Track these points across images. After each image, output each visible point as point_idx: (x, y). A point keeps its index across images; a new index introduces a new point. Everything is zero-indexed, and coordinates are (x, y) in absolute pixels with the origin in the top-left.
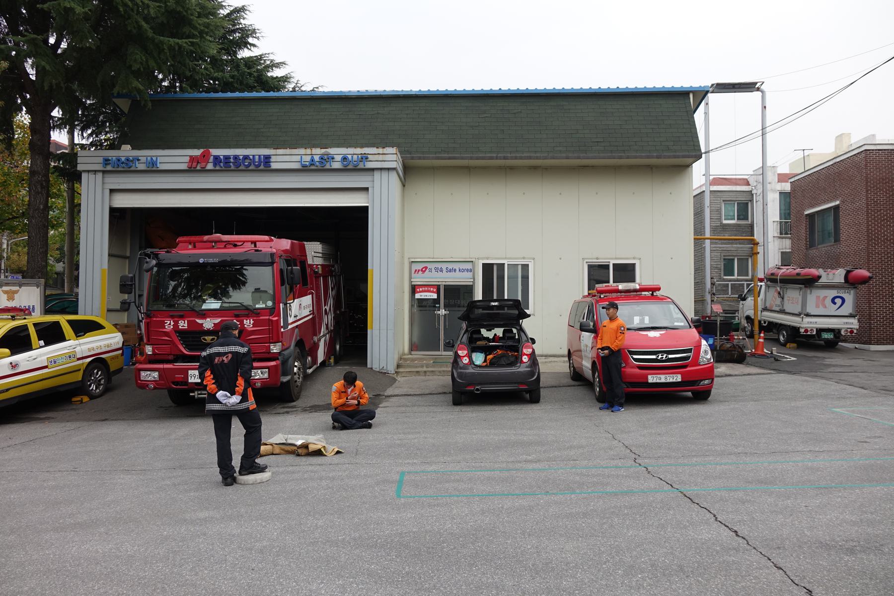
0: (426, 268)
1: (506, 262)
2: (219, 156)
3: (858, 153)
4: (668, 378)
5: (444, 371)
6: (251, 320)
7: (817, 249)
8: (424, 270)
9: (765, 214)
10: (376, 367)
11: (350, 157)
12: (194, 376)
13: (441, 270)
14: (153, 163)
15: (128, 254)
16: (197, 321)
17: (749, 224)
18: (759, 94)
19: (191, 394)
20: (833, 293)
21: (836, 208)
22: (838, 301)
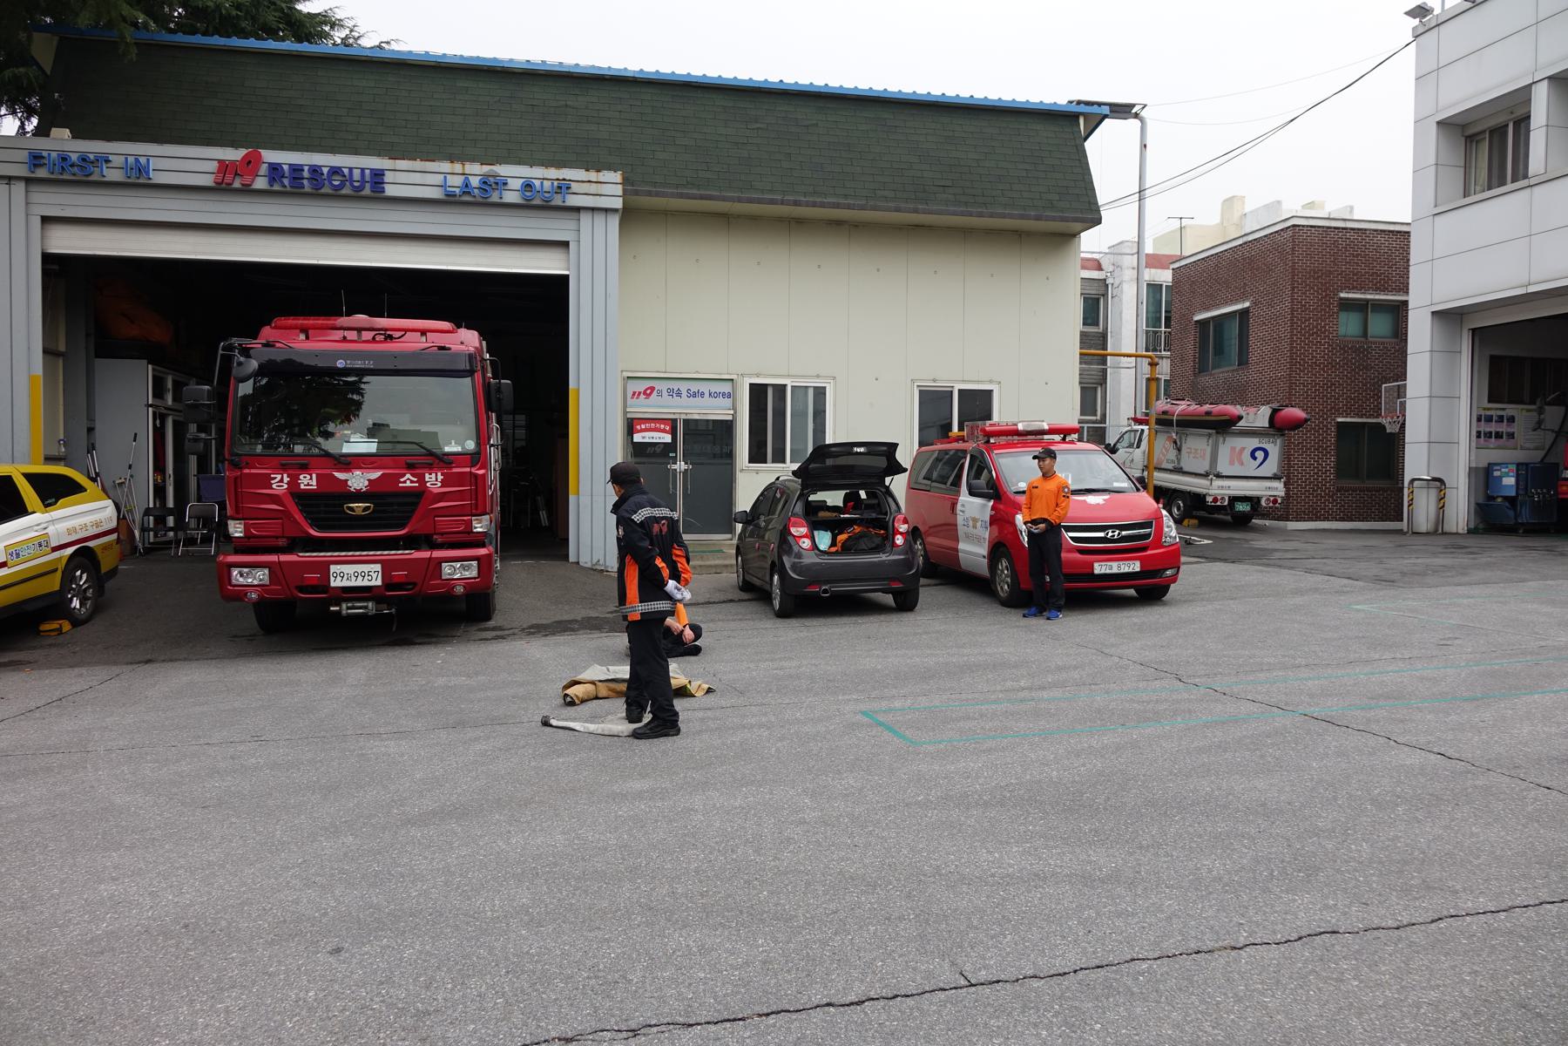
0: (652, 389)
1: (789, 383)
2: (279, 164)
3: (1282, 230)
4: (1122, 567)
5: (700, 566)
6: (439, 474)
7: (1211, 375)
8: (648, 392)
9: (1139, 318)
10: (585, 561)
11: (537, 183)
12: (342, 575)
13: (679, 394)
14: (141, 170)
15: (62, 348)
16: (337, 474)
17: (1097, 333)
18: (1135, 123)
19: (332, 609)
20: (1254, 442)
21: (1244, 313)
22: (1260, 455)
